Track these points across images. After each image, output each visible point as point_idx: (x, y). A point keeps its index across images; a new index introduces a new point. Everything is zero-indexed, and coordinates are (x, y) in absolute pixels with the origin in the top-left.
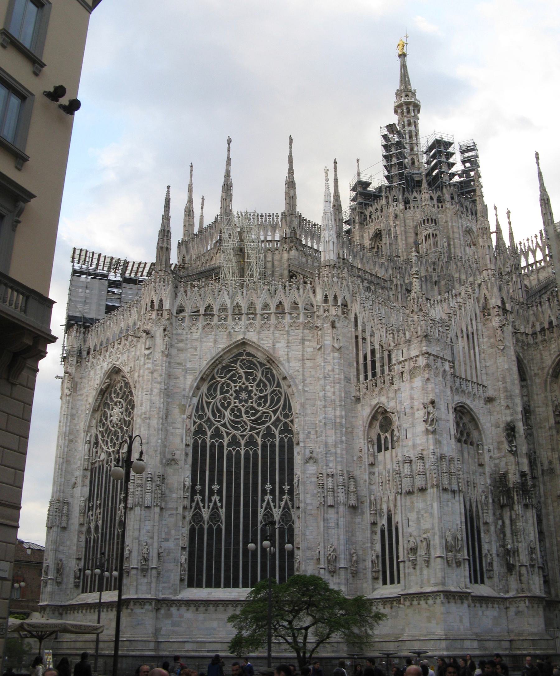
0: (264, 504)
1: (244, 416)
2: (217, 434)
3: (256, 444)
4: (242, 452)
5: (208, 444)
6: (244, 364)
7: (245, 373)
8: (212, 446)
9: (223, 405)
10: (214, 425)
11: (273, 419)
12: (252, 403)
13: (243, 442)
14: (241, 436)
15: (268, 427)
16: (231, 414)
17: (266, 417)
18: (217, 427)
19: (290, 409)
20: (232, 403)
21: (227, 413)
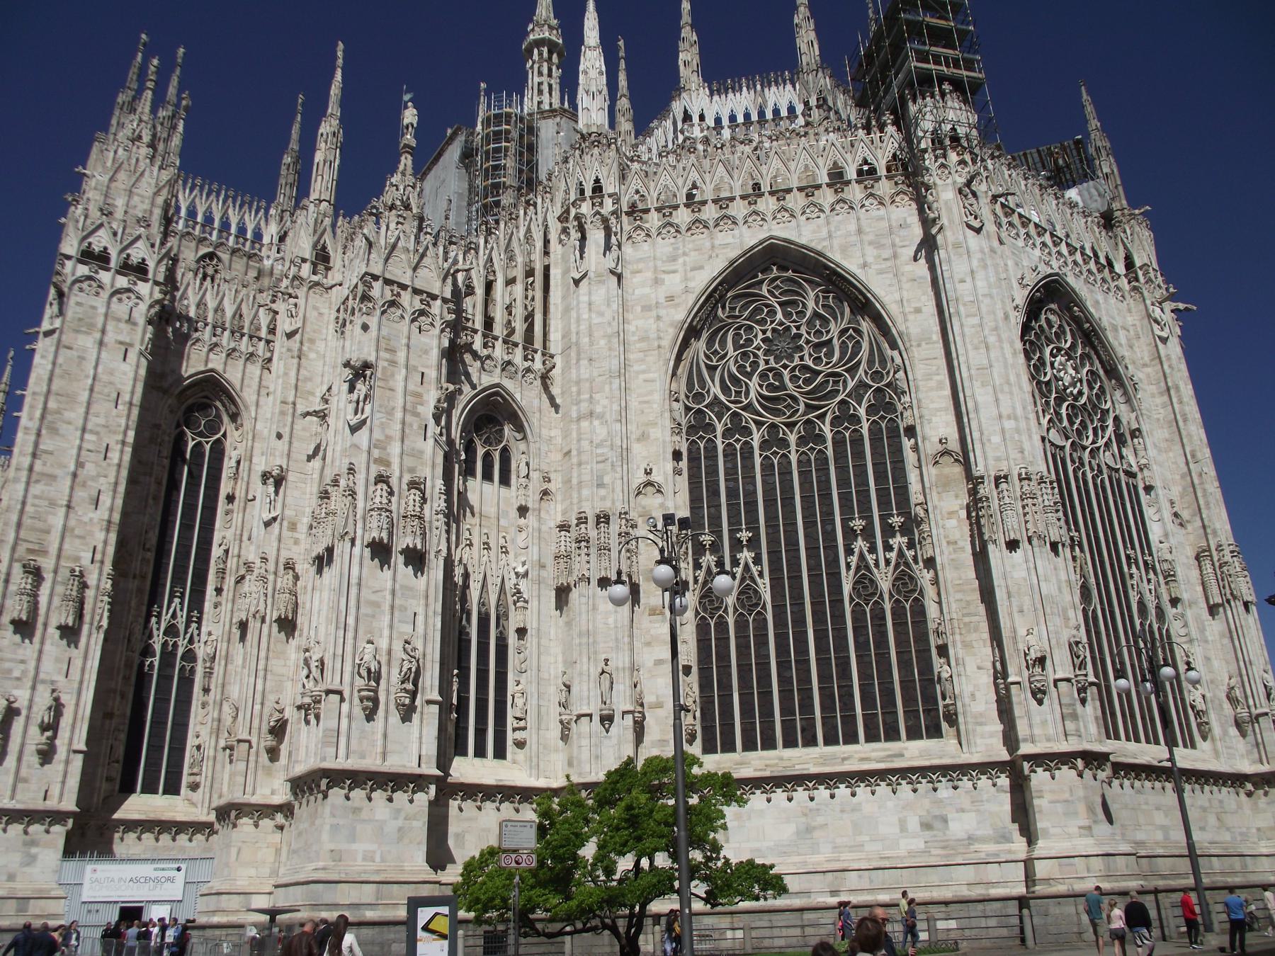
0: (854, 560)
1: (790, 385)
2: (737, 428)
3: (820, 438)
4: (794, 458)
5: (720, 447)
6: (777, 287)
7: (780, 304)
8: (730, 453)
9: (741, 368)
10: (729, 409)
11: (851, 384)
12: (802, 358)
13: (792, 438)
14: (788, 425)
15: (843, 402)
16: (761, 386)
17: (836, 383)
18: (735, 414)
19: (883, 361)
20: (762, 363)
21: (754, 383)
